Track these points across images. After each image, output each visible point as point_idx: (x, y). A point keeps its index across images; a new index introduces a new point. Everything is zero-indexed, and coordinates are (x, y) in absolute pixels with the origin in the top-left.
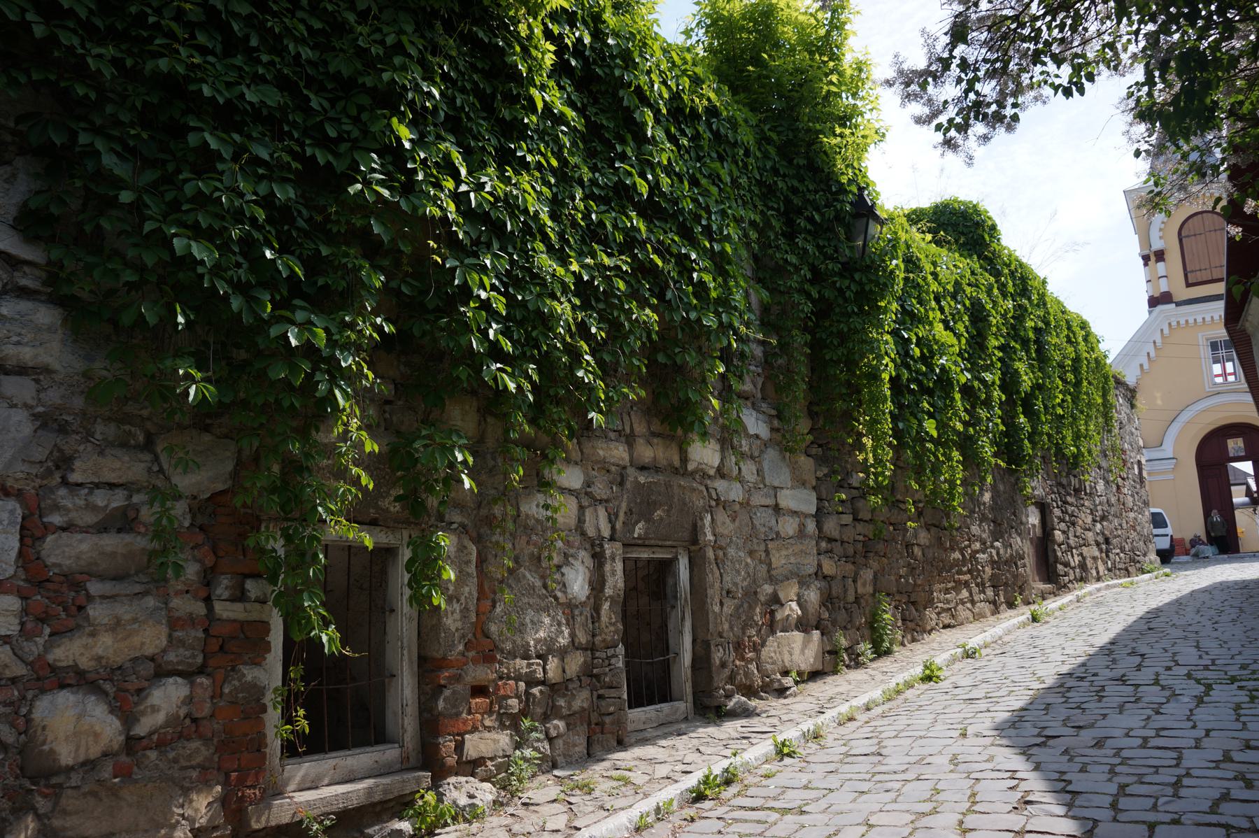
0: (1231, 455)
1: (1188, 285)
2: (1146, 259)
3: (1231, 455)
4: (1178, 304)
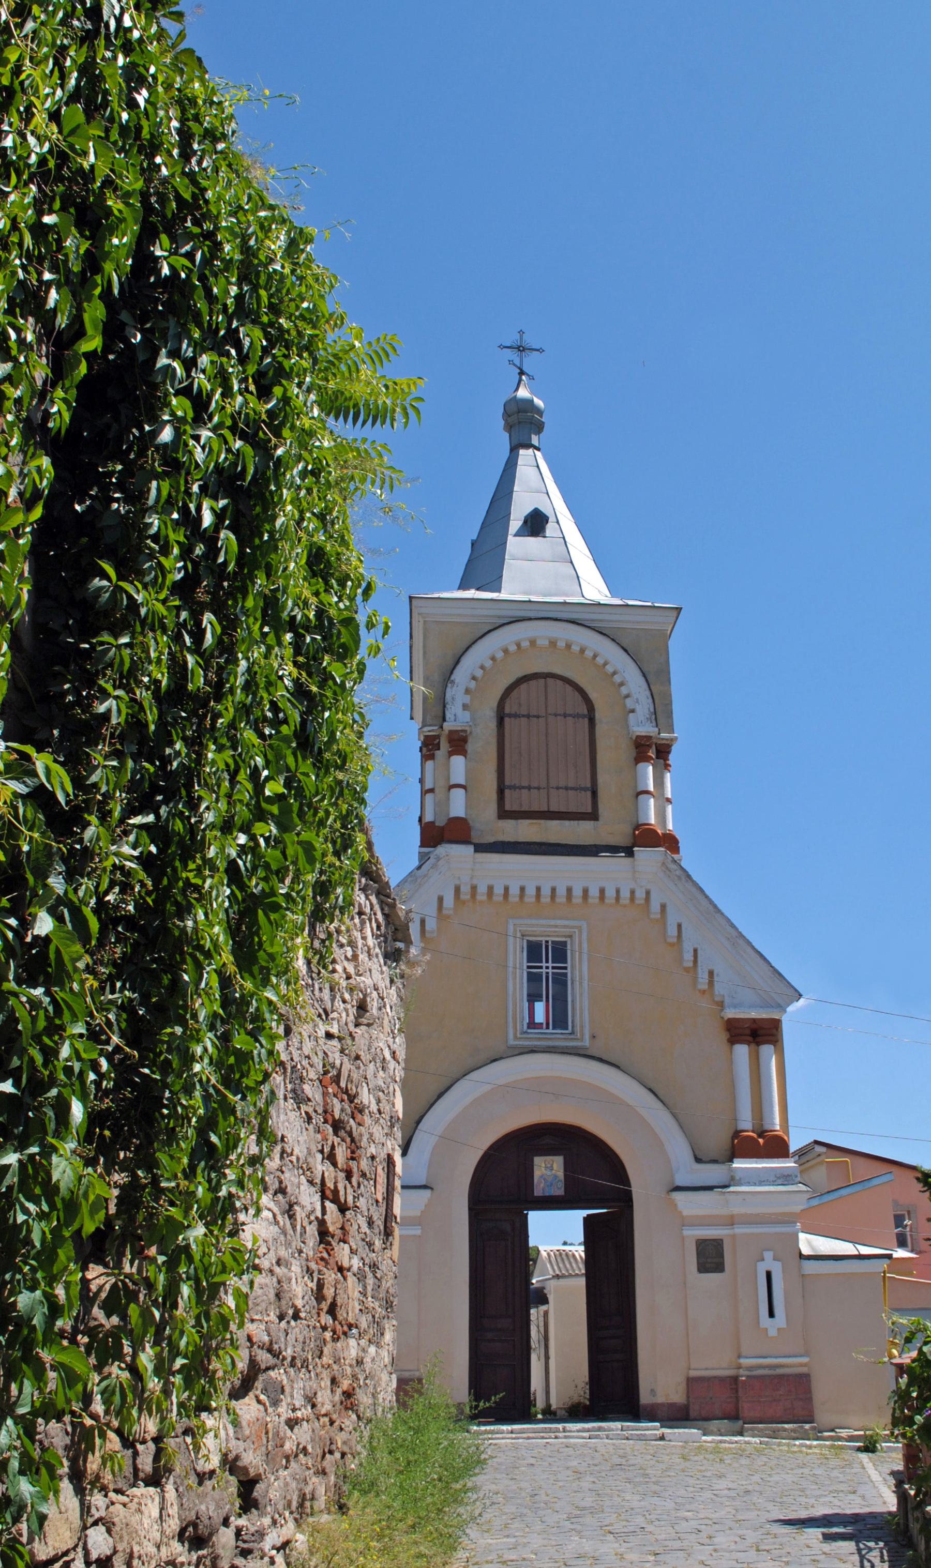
0: (538, 1192)
1: (504, 814)
2: (429, 747)
3: (538, 1192)
4: (481, 848)
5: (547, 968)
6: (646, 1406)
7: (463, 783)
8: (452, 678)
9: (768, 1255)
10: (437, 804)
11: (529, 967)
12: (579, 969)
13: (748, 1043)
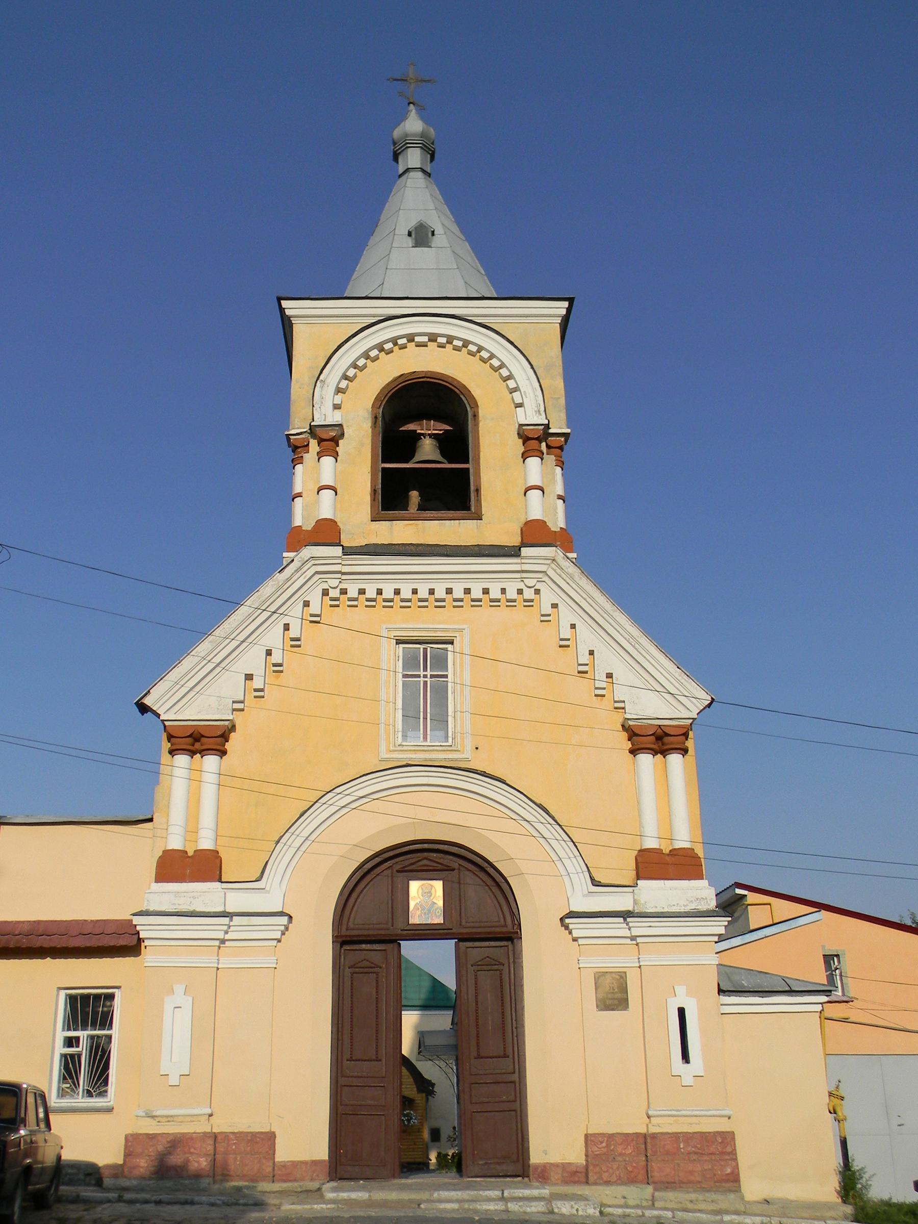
5: (425, 676)
6: (536, 1167)
7: (330, 483)
8: (322, 377)
9: (681, 990)
10: (305, 508)
11: (405, 676)
12: (459, 670)
13: (655, 752)
